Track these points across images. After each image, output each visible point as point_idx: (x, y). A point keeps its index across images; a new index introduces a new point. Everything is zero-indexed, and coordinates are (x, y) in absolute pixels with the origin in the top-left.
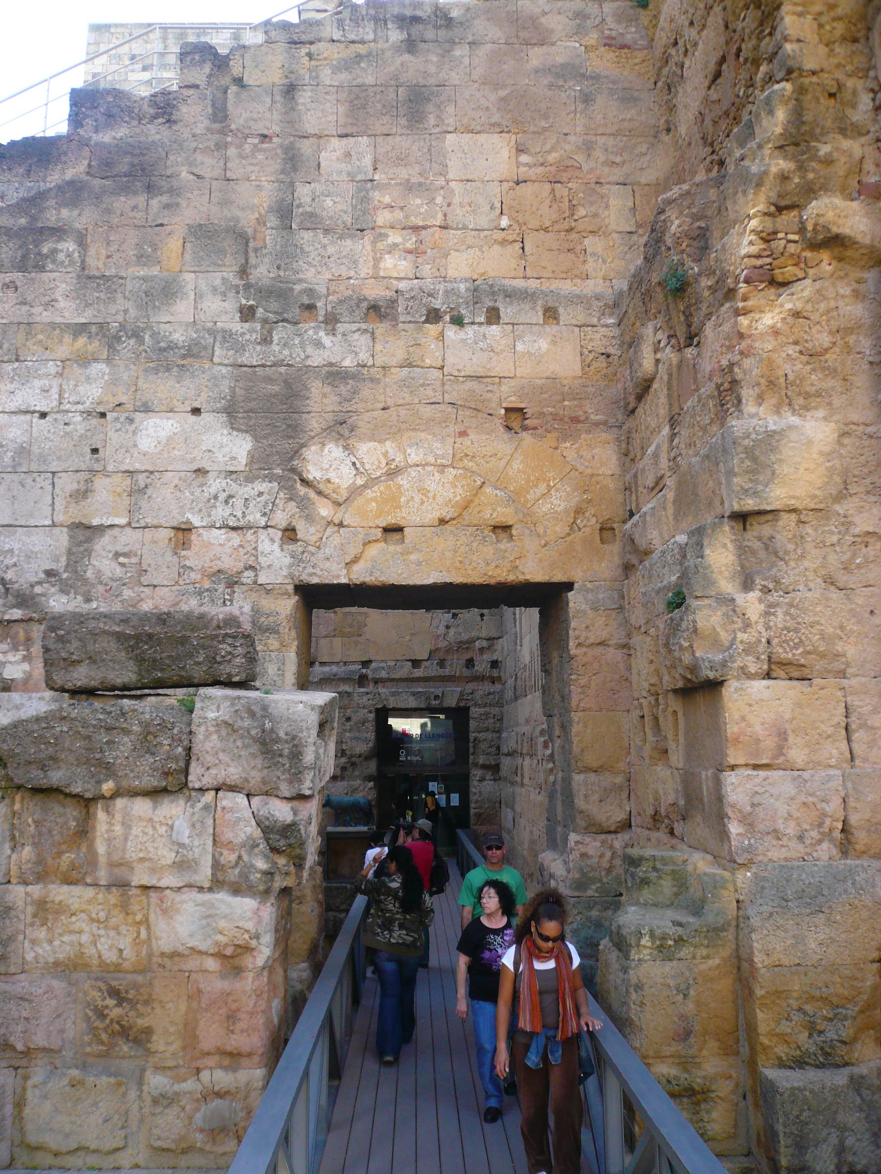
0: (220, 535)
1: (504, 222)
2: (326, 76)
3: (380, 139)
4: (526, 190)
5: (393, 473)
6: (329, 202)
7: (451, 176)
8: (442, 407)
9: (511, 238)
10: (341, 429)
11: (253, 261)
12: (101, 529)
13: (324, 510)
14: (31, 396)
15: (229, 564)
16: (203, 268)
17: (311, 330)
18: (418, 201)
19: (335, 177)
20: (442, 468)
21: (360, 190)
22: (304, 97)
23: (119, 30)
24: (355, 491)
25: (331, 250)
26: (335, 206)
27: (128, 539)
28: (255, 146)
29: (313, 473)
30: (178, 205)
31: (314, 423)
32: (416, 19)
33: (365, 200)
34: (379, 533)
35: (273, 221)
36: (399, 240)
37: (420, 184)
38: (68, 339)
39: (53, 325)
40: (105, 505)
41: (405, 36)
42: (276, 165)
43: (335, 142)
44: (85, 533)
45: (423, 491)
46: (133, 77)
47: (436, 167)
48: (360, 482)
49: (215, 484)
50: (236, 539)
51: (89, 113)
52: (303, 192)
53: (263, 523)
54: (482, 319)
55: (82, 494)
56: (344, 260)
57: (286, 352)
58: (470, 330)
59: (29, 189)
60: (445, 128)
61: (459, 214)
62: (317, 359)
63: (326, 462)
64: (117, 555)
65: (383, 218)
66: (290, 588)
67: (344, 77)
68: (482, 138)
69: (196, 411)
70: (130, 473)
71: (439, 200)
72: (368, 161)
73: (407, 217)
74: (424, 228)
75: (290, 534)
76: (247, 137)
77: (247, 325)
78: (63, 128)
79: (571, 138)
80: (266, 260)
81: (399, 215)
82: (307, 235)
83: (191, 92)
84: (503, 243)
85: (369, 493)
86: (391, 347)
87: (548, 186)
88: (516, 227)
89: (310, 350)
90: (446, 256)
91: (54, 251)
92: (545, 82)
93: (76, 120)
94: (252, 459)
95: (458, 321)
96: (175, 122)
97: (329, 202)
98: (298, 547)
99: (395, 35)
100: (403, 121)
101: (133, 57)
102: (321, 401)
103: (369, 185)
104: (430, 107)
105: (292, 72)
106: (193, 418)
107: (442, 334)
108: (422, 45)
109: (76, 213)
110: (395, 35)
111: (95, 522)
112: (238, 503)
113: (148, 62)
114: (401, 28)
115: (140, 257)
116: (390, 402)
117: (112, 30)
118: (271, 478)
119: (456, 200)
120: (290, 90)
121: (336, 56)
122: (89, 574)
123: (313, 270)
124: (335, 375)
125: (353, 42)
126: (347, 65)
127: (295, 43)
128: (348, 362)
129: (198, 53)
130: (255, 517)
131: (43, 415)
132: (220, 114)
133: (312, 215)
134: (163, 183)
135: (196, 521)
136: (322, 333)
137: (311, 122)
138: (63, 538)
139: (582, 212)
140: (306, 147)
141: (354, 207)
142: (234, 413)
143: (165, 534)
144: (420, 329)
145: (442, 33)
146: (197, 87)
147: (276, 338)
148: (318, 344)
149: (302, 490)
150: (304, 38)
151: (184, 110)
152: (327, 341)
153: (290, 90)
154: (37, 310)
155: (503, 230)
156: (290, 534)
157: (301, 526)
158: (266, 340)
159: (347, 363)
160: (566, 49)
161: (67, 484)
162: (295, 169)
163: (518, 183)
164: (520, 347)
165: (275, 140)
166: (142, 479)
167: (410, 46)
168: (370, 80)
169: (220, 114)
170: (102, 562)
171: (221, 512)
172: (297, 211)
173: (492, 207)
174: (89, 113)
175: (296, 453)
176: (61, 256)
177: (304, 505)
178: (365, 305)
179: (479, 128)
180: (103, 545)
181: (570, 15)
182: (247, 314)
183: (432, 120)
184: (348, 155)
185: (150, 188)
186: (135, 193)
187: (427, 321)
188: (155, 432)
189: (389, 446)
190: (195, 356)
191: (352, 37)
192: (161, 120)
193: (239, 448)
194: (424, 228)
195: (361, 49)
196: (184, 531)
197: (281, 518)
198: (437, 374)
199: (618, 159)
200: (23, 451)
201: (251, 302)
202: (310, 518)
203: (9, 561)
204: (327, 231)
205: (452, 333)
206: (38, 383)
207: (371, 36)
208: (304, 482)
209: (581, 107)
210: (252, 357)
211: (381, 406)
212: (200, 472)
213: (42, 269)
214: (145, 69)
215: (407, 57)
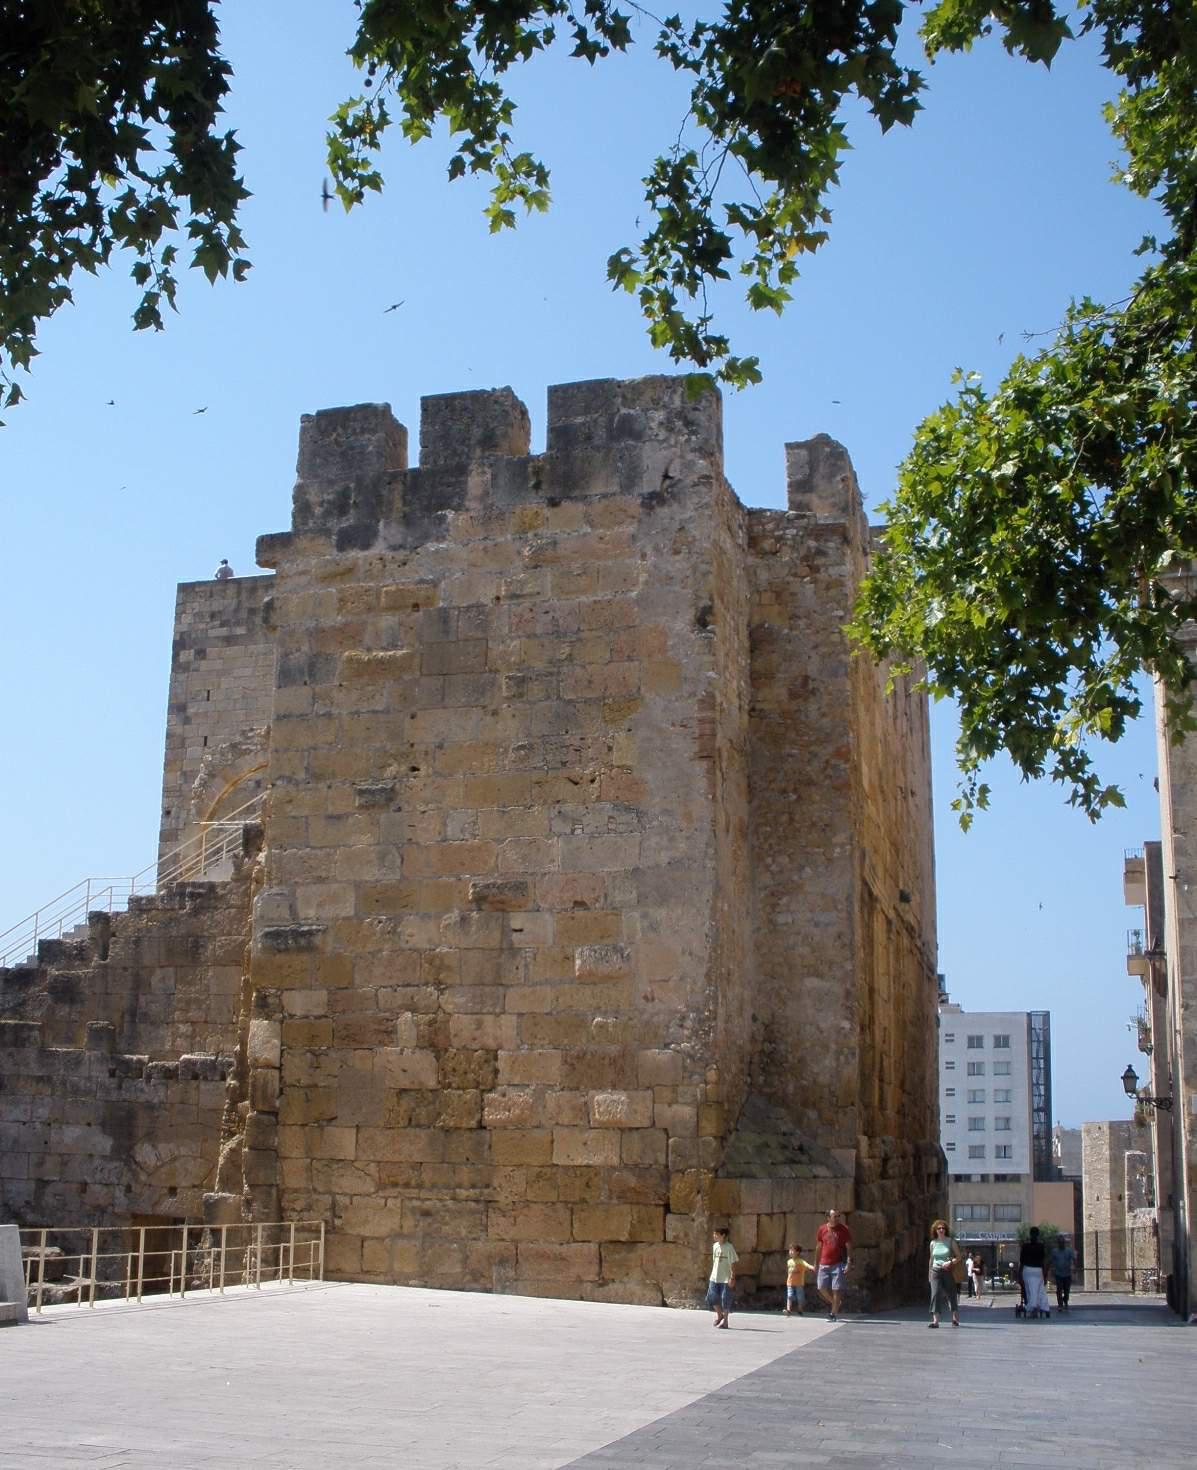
0: (97, 1188)
5: (174, 1159)
10: (151, 1137)
11: (118, 1040)
12: (48, 1182)
13: (143, 1177)
14: (18, 1113)
15: (101, 1202)
17: (141, 1083)
20: (195, 1158)
23: (202, 589)
24: (157, 1168)
25: (153, 1034)
26: (155, 1008)
27: (60, 1187)
29: (139, 1159)
31: (140, 1132)
34: (166, 1191)
35: (127, 1018)
38: (34, 1084)
39: (28, 1076)
40: (50, 1171)
43: (158, 972)
44: (42, 1183)
45: (186, 1170)
48: (159, 1164)
49: (97, 1162)
50: (105, 1190)
52: (142, 999)
53: (116, 1182)
55: (40, 1164)
62: (142, 1098)
63: (145, 1153)
64: (55, 1195)
66: (129, 1216)
69: (89, 1125)
70: (61, 1155)
72: (172, 982)
75: (129, 1189)
78: (35, 964)
82: (142, 1026)
85: (163, 1170)
86: (175, 1090)
89: (139, 1094)
91: (29, 1037)
93: (41, 958)
94: (113, 1147)
98: (131, 1195)
101: (213, 616)
102: (142, 1122)
106: (87, 1128)
107: (198, 1087)
111: (46, 1178)
112: (106, 1171)
113: (224, 618)
117: (197, 589)
118: (121, 1160)
122: (44, 1203)
124: (150, 1107)
128: (156, 1101)
129: (98, 919)
130: (114, 1179)
131: (24, 1123)
133: (145, 1014)
135: (89, 1181)
137: (147, 960)
138: (32, 1185)
140: (142, 972)
142: (105, 1126)
143: (75, 1186)
149: (134, 1167)
154: (22, 1068)
156: (129, 1189)
157: (133, 1185)
158: (120, 1087)
161: (34, 1158)
165: (130, 970)
166: (66, 1158)
168: (174, 933)
170: (49, 1200)
171: (98, 1176)
172: (139, 1011)
173: (229, 1011)
175: (131, 1148)
176: (32, 1039)
177: (135, 1175)
180: (49, 1190)
182: (112, 1074)
184: (164, 978)
185: (72, 1001)
188: (71, 1134)
189: (172, 1145)
191: (168, 907)
193: (105, 1144)
196: (86, 1184)
197: (125, 1180)
198: (194, 1108)
200: (16, 1141)
202: (137, 1181)
203: (10, 1195)
204: (152, 1023)
205: (203, 1086)
206: (23, 1107)
208: (136, 1162)
210: (114, 1096)
212: (91, 1156)
213: (24, 1046)
214: (222, 625)
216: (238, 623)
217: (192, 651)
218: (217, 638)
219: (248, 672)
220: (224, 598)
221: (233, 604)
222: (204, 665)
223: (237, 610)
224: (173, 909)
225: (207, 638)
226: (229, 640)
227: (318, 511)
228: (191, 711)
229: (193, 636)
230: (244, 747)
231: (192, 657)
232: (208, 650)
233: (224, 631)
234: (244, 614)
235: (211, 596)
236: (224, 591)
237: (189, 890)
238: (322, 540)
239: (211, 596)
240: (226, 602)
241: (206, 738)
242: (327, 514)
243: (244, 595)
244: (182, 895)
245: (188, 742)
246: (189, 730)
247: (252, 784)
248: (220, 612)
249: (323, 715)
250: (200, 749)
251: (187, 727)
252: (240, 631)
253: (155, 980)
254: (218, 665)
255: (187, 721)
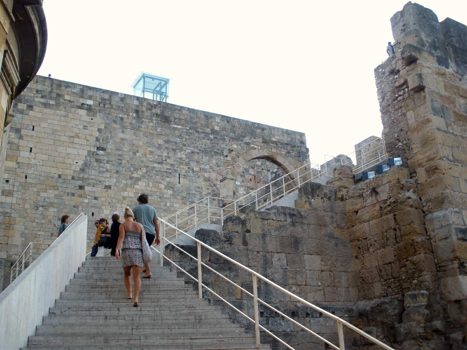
1: (320, 284)
2: (273, 233)
3: (288, 255)
4: (324, 273)
6: (276, 275)
7: (306, 268)
8: (311, 343)
9: (321, 289)
16: (249, 299)
18: (299, 276)
19: (277, 267)
21: (284, 272)
22: (268, 239)
28: (256, 255)
30: (238, 275)
32: (294, 215)
33: (285, 275)
36: (295, 289)
37: (299, 271)
41: (291, 220)
42: (262, 262)
43: (276, 256)
46: (37, 99)
47: (303, 266)
51: (207, 238)
54: (318, 316)
56: (282, 295)
57: (273, 327)
58: (316, 319)
59: (193, 265)
60: (304, 253)
61: (309, 281)
65: (291, 281)
67: (277, 233)
68: (313, 256)
71: (304, 276)
72: (285, 261)
73: (296, 282)
74: (301, 285)
76: (253, 251)
77: (262, 318)
79: (333, 257)
80: (262, 295)
81: (294, 281)
83: (236, 234)
84: (320, 290)
87: (328, 272)
88: (322, 285)
89: (279, 326)
90: (307, 294)
92: (326, 239)
95: (312, 317)
96: (232, 244)
97: (276, 275)
99: (289, 220)
100: (293, 249)
101: (37, 91)
103: (286, 270)
104: (300, 245)
105: (263, 230)
108: (296, 224)
109: (209, 276)
110: (289, 220)
114: (290, 217)
115: (229, 293)
116: (299, 342)
119: (308, 277)
120: (264, 236)
121: (275, 225)
123: (274, 298)
125: (279, 221)
126: (278, 229)
127: (263, 219)
132: (245, 243)
134: (234, 267)
136: (281, 321)
139: (336, 281)
140: (268, 255)
141: (283, 278)
144: (305, 319)
145: (300, 219)
146: (238, 232)
147: (270, 322)
148: (281, 324)
150: (266, 218)
151: (235, 240)
152: (283, 324)
153: (264, 236)
155: (319, 286)
159: (288, 331)
160: (331, 228)
162: (266, 264)
163: (322, 271)
164: (327, 324)
165: (261, 253)
167: (293, 224)
169: (245, 243)
173: (317, 279)
174: (207, 238)
178: (291, 312)
179: (312, 253)
181: (330, 217)
183: (301, 249)
184: (279, 259)
186: (226, 270)
187: (306, 317)
190: (250, 329)
191: (279, 219)
192: (228, 242)
194: (301, 285)
195: (281, 224)
199: (344, 264)
201: (263, 311)
207: (283, 220)
209: (335, 248)
211: (297, 344)
214: (42, 97)
215: (292, 228)
216: (51, 98)
217: (25, 105)
218: (40, 102)
219: (56, 122)
220: (44, 85)
221: (49, 89)
222: (31, 113)
223: (51, 92)
224: (280, 221)
225: (33, 101)
226: (46, 105)
227: (427, 45)
228: (23, 132)
229: (26, 98)
230: (252, 146)
231: (25, 108)
232: (34, 107)
233: (43, 100)
234: (54, 95)
235: (37, 82)
236: (44, 82)
237: (288, 211)
238: (432, 57)
239: (37, 82)
240: (45, 87)
241: (31, 148)
242: (430, 47)
243: (55, 86)
244: (285, 214)
245: (20, 148)
246: (22, 143)
247: (56, 176)
248: (41, 91)
249: (452, 133)
250: (28, 153)
251: (20, 140)
252: (52, 102)
253: (275, 260)
254: (40, 115)
255: (21, 138)
